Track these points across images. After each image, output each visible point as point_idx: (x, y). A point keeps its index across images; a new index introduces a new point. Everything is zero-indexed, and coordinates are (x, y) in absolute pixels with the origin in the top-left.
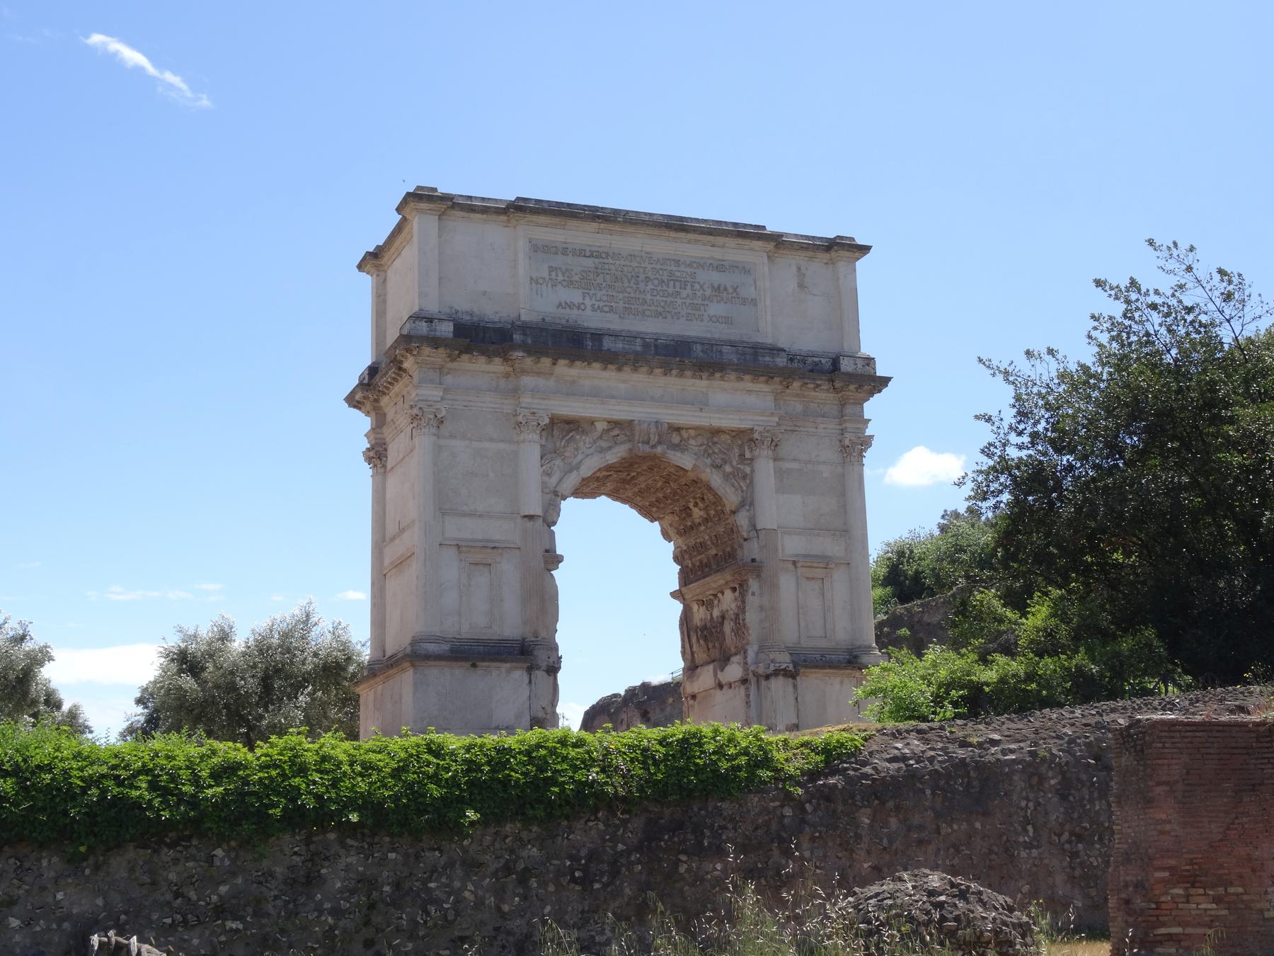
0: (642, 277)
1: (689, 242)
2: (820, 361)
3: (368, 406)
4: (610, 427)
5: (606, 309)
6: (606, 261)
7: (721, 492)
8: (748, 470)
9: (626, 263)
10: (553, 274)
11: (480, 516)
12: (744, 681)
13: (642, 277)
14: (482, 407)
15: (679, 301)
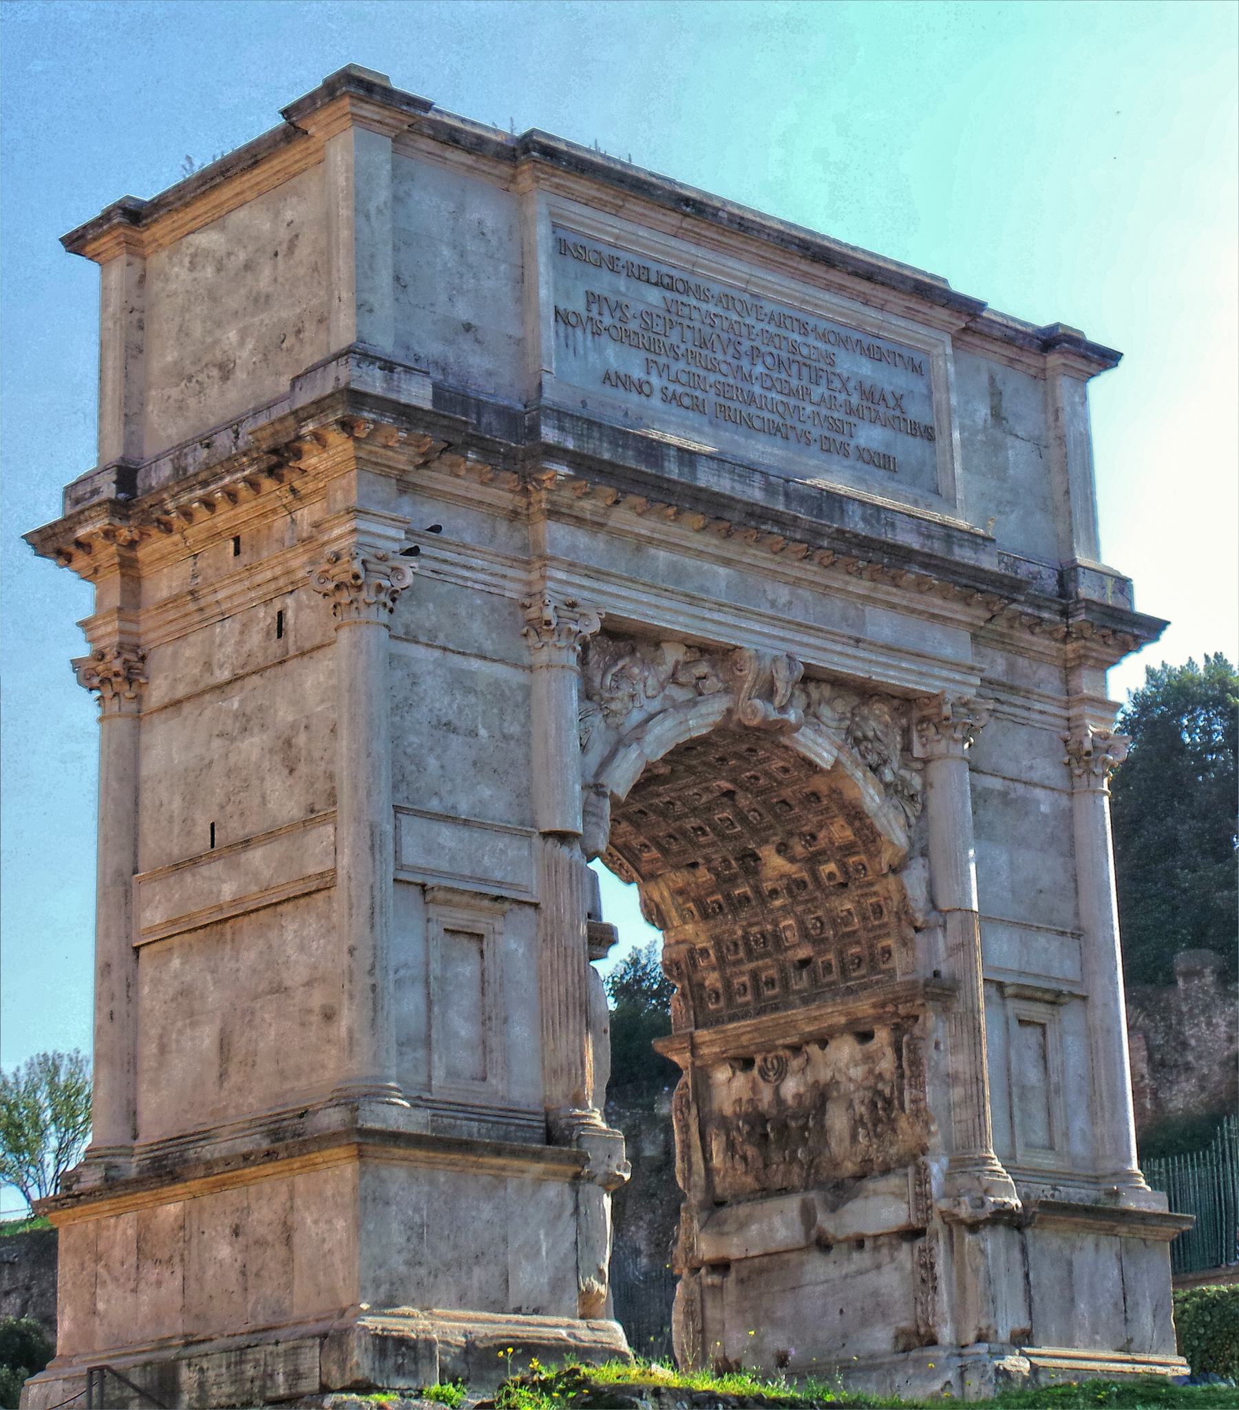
0: (746, 345)
1: (828, 287)
2: (1039, 572)
3: (107, 553)
4: (688, 658)
5: (686, 401)
6: (684, 299)
7: (880, 824)
8: (917, 781)
9: (719, 311)
10: (595, 308)
11: (466, 823)
12: (912, 1234)
13: (746, 345)
14: (466, 579)
15: (809, 409)
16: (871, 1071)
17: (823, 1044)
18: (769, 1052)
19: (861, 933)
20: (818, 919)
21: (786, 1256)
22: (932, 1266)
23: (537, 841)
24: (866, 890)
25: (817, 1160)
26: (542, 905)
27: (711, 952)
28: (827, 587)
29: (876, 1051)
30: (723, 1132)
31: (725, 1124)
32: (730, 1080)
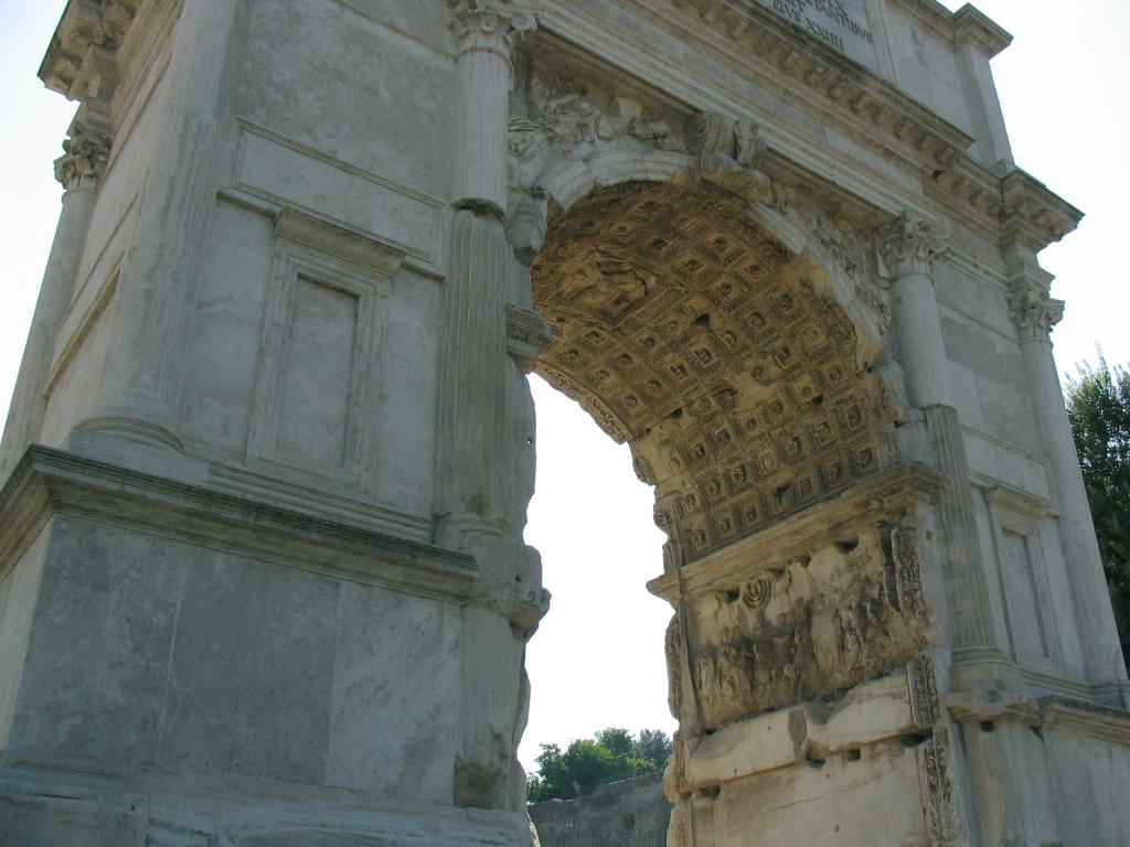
12: (913, 737)
16: (856, 578)
17: (806, 561)
18: (753, 578)
19: (839, 442)
20: (796, 439)
21: (775, 774)
22: (943, 769)
23: (448, 213)
24: (840, 397)
25: (804, 676)
26: (447, 280)
27: (696, 497)
28: (786, 91)
29: (860, 557)
30: (710, 661)
31: (712, 652)
32: (716, 612)
